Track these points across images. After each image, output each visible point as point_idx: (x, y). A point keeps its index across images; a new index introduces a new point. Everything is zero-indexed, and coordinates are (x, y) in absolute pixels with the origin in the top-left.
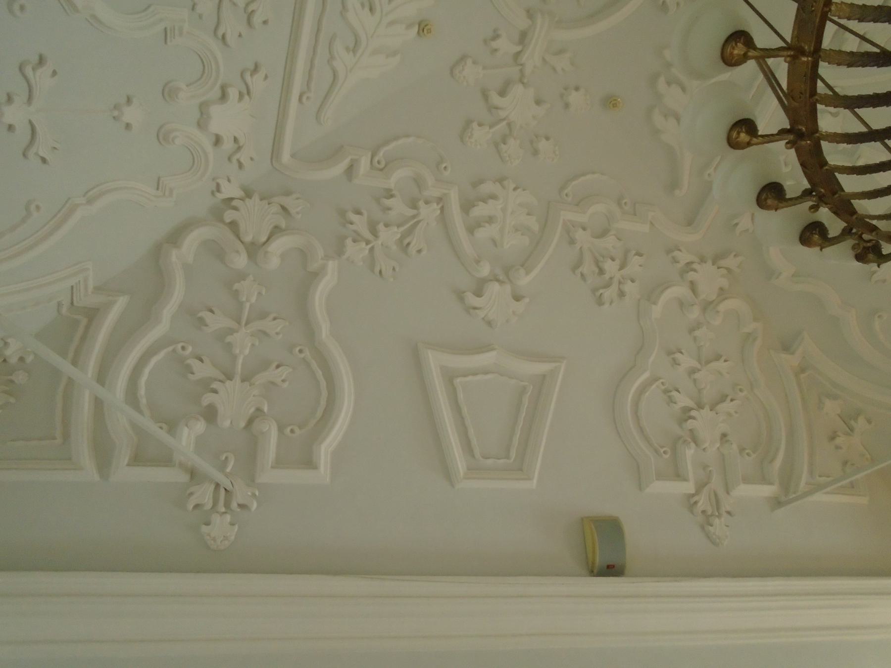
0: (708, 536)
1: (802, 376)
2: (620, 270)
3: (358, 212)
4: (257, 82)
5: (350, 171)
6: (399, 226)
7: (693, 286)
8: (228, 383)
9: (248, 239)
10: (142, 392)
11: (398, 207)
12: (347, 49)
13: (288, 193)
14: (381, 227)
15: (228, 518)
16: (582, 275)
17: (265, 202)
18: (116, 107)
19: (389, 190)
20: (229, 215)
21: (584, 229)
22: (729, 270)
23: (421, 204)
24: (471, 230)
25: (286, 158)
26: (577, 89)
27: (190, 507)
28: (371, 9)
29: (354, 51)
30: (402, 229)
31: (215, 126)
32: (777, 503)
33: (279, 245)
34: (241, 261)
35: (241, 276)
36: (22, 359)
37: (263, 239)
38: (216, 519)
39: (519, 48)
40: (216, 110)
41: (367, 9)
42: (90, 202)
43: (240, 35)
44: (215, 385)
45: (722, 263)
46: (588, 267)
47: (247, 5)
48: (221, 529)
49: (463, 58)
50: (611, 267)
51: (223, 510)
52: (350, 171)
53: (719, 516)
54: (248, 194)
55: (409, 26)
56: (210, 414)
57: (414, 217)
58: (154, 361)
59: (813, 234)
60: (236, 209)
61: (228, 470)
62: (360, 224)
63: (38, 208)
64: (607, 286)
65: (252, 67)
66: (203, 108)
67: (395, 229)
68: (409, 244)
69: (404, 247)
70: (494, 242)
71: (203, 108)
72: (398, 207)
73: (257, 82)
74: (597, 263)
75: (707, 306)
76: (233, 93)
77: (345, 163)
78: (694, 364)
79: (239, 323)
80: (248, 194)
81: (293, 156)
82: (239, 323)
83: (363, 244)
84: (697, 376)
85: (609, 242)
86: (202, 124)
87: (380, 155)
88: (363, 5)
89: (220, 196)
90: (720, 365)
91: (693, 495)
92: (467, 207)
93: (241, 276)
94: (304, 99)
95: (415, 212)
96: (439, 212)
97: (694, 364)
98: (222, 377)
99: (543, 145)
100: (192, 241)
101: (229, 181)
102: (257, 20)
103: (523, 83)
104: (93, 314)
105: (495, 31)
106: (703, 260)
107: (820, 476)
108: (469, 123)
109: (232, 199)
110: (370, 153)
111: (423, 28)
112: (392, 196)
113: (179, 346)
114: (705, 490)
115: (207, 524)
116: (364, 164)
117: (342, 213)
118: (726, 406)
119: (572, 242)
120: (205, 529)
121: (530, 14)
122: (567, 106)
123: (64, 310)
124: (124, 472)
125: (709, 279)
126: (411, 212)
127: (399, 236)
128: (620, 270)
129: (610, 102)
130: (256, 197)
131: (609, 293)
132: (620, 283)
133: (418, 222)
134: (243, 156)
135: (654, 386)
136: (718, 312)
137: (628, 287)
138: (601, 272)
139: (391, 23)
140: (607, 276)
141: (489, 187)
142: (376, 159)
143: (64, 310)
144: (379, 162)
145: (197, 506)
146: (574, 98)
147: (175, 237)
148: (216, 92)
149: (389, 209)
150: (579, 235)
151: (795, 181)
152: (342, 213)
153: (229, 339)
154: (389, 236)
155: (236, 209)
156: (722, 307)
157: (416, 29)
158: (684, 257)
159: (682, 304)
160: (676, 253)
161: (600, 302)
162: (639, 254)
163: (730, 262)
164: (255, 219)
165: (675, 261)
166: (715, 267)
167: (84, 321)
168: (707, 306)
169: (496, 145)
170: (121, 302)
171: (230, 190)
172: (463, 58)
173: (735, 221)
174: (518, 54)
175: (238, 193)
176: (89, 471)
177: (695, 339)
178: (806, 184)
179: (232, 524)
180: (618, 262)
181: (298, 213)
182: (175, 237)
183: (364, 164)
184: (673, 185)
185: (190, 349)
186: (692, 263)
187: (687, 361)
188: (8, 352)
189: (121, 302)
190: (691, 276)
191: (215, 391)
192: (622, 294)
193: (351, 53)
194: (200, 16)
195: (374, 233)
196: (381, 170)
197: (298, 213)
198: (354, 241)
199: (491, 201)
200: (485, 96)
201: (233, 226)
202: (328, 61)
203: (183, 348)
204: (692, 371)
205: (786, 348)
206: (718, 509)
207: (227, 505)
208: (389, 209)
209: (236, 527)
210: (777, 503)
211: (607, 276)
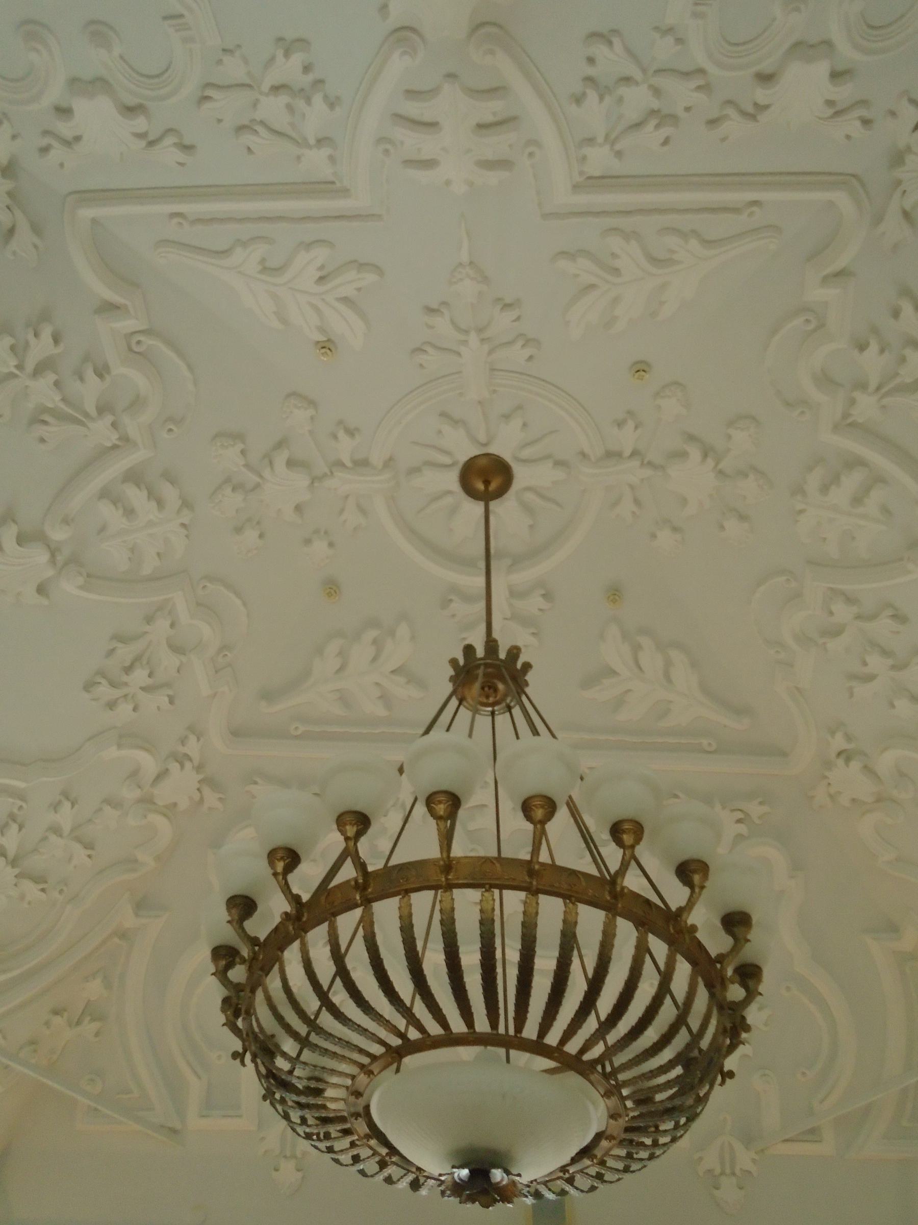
1: (116, 940)
2: (142, 689)
4: (168, 153)
5: (109, 308)
6: (63, 400)
11: (90, 390)
12: (263, 261)
13: (36, 229)
14: (51, 377)
16: (113, 650)
17: (8, 201)
21: (172, 625)
23: (109, 419)
24: (105, 494)
25: (87, 213)
26: (331, 545)
29: (265, 270)
30: (62, 405)
31: (81, 106)
39: (349, 464)
40: (104, 105)
41: (319, 274)
43: (220, 121)
45: (207, 791)
46: (125, 653)
47: (262, 123)
49: (312, 403)
50: (140, 676)
52: (109, 308)
55: (321, 330)
57: (87, 415)
59: (224, 956)
62: (41, 347)
64: (113, 685)
65: (187, 142)
67: (57, 398)
68: (44, 422)
69: (38, 418)
70: (103, 529)
71: (98, 85)
72: (90, 390)
73: (168, 153)
74: (138, 659)
75: (147, 801)
76: (140, 123)
77: (117, 299)
78: (67, 829)
81: (94, 221)
83: (13, 362)
84: (53, 838)
85: (168, 662)
88: (322, 268)
90: (80, 852)
92: (133, 477)
94: (175, 220)
95: (93, 412)
96: (109, 444)
97: (67, 829)
99: (251, 535)
101: (14, 137)
102: (248, 139)
103: (312, 483)
105: (357, 429)
106: (199, 768)
108: (238, 437)
111: (327, 346)
112: (100, 376)
116: (127, 324)
117: (45, 316)
118: (29, 887)
119: (149, 620)
121: (389, 463)
122: (308, 542)
125: (180, 786)
126: (90, 407)
127: (50, 405)
128: (142, 689)
129: (332, 588)
131: (104, 690)
132: (126, 696)
133: (82, 424)
134: (58, 152)
135: (11, 800)
136: (145, 817)
137: (125, 709)
138: (128, 670)
140: (125, 678)
141: (170, 493)
142: (142, 338)
144: (139, 342)
146: (320, 546)
148: (132, 101)
149: (82, 379)
150: (162, 625)
151: (261, 926)
152: (45, 316)
154: (42, 390)
157: (322, 338)
158: (193, 748)
159: (134, 774)
160: (192, 739)
161: (88, 686)
162: (171, 701)
163: (211, 798)
165: (183, 741)
166: (198, 786)
169: (228, 480)
173: (258, 780)
174: (340, 464)
178: (262, 937)
180: (149, 681)
181: (14, 253)
183: (127, 324)
184: (268, 696)
186: (190, 760)
187: (66, 817)
190: (174, 767)
192: (111, 705)
193: (260, 267)
194: (220, 62)
195: (38, 372)
196: (130, 349)
197: (14, 253)
198: (13, 348)
199: (154, 504)
200: (281, 444)
202: (238, 240)
204: (56, 830)
205: (141, 906)
208: (82, 379)
211: (125, 678)
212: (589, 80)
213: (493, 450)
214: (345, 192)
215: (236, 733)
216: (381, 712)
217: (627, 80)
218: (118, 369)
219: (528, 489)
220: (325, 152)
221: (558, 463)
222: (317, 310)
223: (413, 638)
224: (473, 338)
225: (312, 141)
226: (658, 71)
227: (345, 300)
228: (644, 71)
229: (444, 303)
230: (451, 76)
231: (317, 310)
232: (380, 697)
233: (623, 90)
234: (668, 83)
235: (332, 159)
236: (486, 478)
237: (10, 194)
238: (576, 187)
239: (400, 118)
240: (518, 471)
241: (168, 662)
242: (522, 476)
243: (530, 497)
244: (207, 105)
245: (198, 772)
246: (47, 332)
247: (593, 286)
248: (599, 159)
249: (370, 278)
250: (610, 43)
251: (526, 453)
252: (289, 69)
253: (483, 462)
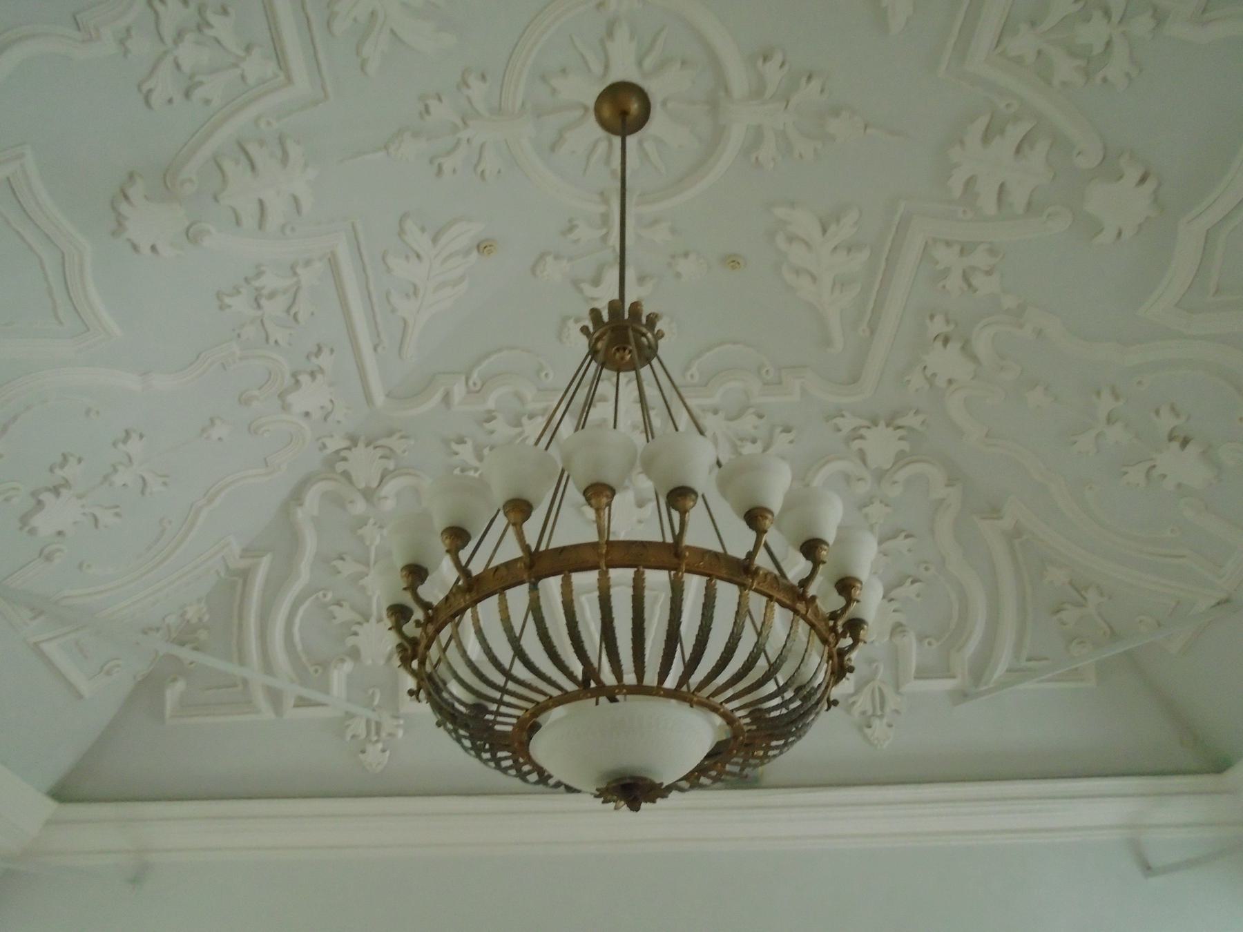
0: (865, 737)
3: (461, 441)
4: (325, 360)
5: (447, 398)
7: (862, 456)
8: (366, 625)
9: (362, 486)
10: (297, 638)
12: (407, 295)
13: (390, 434)
14: (486, 451)
15: (380, 746)
18: (204, 430)
19: (490, 411)
20: (341, 466)
21: (716, 412)
22: (911, 429)
23: (525, 420)
26: (686, 255)
27: (348, 738)
28: (418, 256)
29: (415, 293)
32: (963, 696)
33: (391, 487)
34: (360, 507)
35: (362, 522)
36: (200, 619)
37: (374, 485)
38: (370, 748)
39: (604, 231)
42: (210, 501)
44: (355, 628)
48: (375, 757)
49: (542, 256)
51: (375, 738)
53: (881, 717)
54: (354, 441)
55: (467, 253)
56: (355, 654)
57: (520, 434)
58: (301, 612)
60: (344, 459)
61: (376, 702)
63: (170, 522)
65: (315, 349)
66: (281, 396)
75: (880, 476)
77: (438, 396)
79: (367, 564)
80: (354, 441)
82: (367, 564)
85: (748, 423)
86: (285, 408)
87: (475, 375)
88: (407, 257)
89: (329, 451)
91: (852, 695)
93: (362, 522)
95: (518, 430)
98: (358, 618)
100: (312, 496)
104: (245, 575)
105: (570, 221)
107: (1029, 660)
109: (337, 452)
110: (463, 378)
113: (320, 594)
114: (867, 690)
115: (363, 752)
116: (459, 391)
120: (361, 756)
123: (222, 574)
124: (291, 713)
125: (881, 445)
129: (733, 261)
130: (361, 444)
139: (445, 260)
142: (471, 383)
143: (222, 574)
144: (475, 384)
145: (353, 737)
146: (683, 266)
147: (296, 497)
153: (362, 582)
155: (344, 459)
156: (902, 475)
158: (847, 423)
160: (839, 421)
162: (787, 430)
164: (364, 466)
166: (890, 429)
167: (240, 581)
168: (880, 476)
170: (265, 562)
171: (334, 444)
172: (542, 256)
173: (907, 378)
175: (346, 444)
176: (268, 714)
177: (866, 516)
179: (383, 751)
181: (404, 451)
182: (296, 497)
183: (459, 391)
185: (330, 595)
188: (188, 616)
189: (265, 562)
191: (356, 634)
196: (478, 392)
197: (404, 451)
201: (346, 475)
203: (325, 596)
206: (882, 708)
207: (378, 733)
209: (388, 753)
210: (963, 696)
212: (187, 94)
213: (591, 103)
214: (333, 254)
215: (855, 380)
216: (864, 255)
217: (178, 66)
218: (491, 404)
219: (640, 63)
220: (299, 270)
221: (610, 34)
222: (451, 256)
223: (792, 205)
224: (464, 135)
225: (295, 279)
226: (162, 40)
227: (435, 240)
228: (166, 53)
229: (431, 162)
230: (216, 199)
231: (451, 256)
232: (849, 250)
233: (186, 67)
234: (168, 32)
235: (308, 263)
236: (623, 109)
237: (367, 445)
238: (289, 80)
239: (261, 224)
240: (616, 76)
241: (748, 423)
242: (624, 71)
243: (648, 63)
244: (300, 317)
245: (876, 425)
246: (455, 447)
247: (392, 31)
248: (258, 67)
249: (409, 225)
250: (150, 91)
251: (597, 68)
252: (240, 305)
253: (607, 112)
